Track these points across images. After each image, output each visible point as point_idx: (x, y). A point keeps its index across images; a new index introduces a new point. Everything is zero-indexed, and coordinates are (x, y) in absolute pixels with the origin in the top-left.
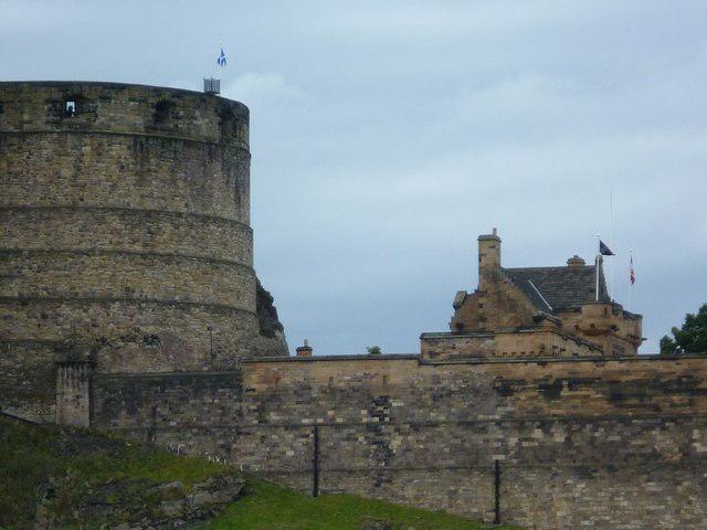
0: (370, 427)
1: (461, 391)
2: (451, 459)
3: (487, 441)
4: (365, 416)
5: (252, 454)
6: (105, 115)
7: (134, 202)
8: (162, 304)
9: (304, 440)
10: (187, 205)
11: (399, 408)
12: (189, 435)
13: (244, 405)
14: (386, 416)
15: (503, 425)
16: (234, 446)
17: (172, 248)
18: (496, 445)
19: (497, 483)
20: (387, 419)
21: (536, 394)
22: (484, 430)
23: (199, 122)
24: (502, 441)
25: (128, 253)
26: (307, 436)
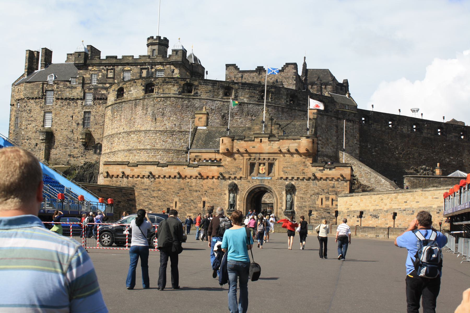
25: (105, 154)
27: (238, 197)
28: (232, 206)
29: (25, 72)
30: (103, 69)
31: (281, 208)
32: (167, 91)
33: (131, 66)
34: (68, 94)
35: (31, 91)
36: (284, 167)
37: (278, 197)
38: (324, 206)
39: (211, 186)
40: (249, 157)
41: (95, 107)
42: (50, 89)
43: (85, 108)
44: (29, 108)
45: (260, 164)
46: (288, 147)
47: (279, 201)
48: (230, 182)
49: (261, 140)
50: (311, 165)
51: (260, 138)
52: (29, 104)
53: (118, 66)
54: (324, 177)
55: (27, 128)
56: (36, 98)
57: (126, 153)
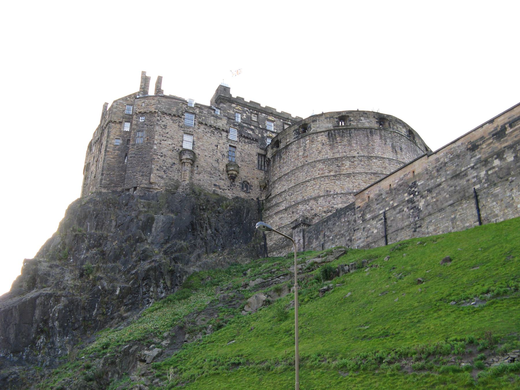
0: (411, 201)
1: (451, 160)
2: (450, 200)
3: (468, 180)
4: (406, 197)
5: (360, 239)
6: (314, 127)
7: (330, 155)
8: (345, 194)
9: (380, 222)
10: (358, 153)
11: (422, 184)
12: (336, 240)
13: (356, 216)
14: (416, 192)
15: (475, 167)
16: (353, 238)
17: (351, 171)
18: (473, 180)
19: (477, 202)
20: (417, 193)
21: (491, 141)
22: (466, 175)
23: (364, 121)
24: (477, 176)
25: (327, 176)
26: (382, 219)
29: (141, 91)
30: (247, 111)
32: (399, 129)
33: (275, 117)
34: (213, 122)
35: (167, 106)
41: (240, 143)
42: (191, 111)
43: (230, 141)
44: (163, 123)
52: (164, 119)
53: (262, 113)
55: (160, 144)
56: (174, 115)
57: (370, 176)
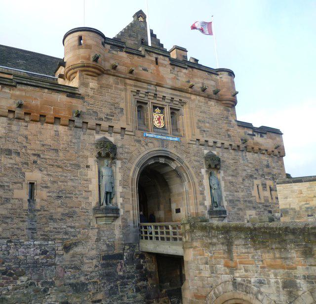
27: (119, 177)
28: (110, 195)
31: (203, 204)
36: (199, 121)
37: (196, 180)
38: (263, 201)
39: (49, 141)
40: (135, 89)
45: (155, 107)
46: (203, 84)
47: (199, 189)
48: (98, 137)
49: (156, 59)
50: (236, 123)
51: (155, 55)
54: (256, 148)
